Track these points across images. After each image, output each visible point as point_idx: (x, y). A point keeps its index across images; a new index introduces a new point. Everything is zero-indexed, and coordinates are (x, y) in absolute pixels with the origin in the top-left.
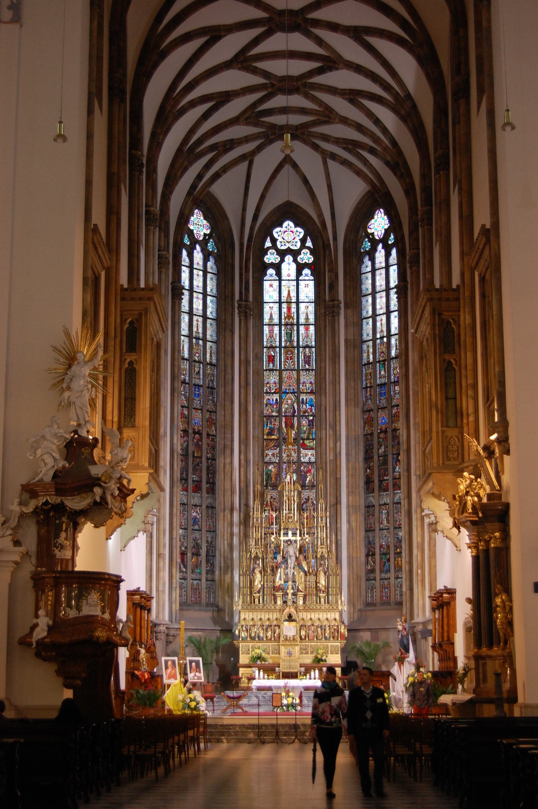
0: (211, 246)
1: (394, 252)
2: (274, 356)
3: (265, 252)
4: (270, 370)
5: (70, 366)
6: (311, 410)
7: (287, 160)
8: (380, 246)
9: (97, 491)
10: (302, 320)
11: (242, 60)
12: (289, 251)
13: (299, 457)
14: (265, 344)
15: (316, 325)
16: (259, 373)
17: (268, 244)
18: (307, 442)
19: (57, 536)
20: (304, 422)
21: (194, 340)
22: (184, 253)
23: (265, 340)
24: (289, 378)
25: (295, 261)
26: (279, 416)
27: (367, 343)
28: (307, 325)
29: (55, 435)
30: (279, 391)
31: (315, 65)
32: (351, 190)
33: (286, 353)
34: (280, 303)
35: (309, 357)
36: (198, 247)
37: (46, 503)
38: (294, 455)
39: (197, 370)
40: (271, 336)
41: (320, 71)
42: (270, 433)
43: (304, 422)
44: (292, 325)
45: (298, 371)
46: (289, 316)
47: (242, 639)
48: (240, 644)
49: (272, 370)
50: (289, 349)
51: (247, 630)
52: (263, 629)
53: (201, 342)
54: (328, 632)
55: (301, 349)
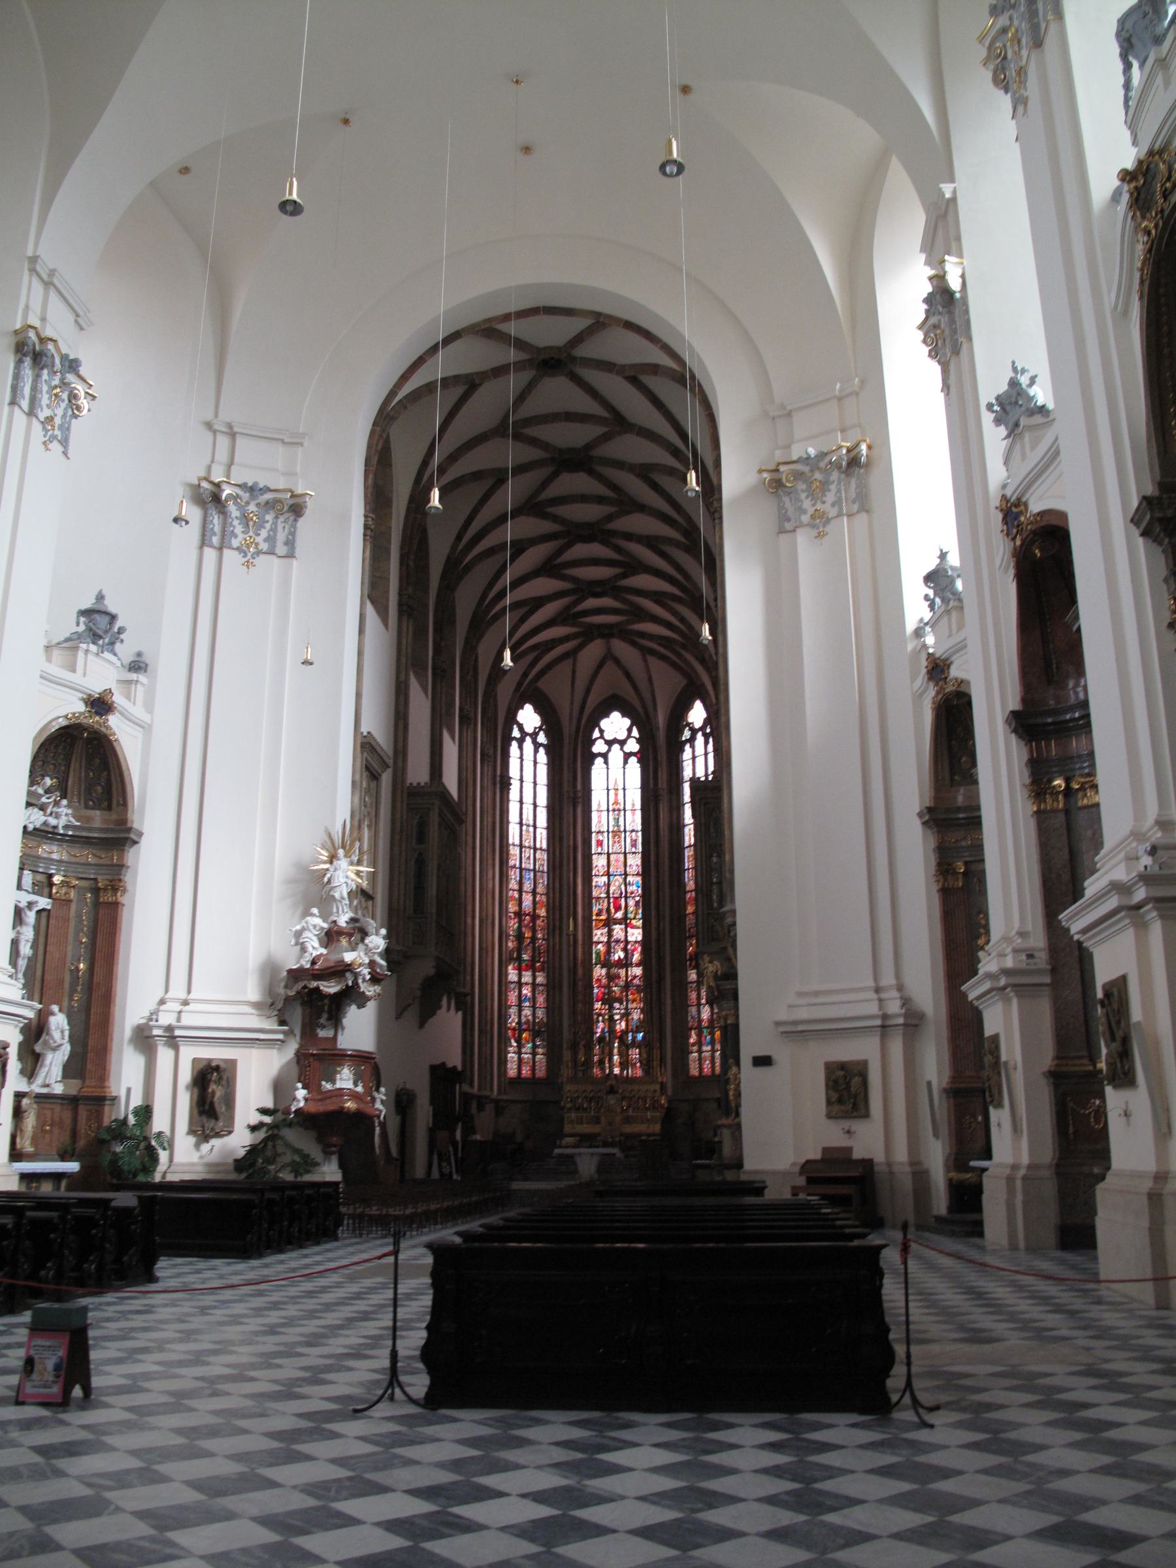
0: (542, 738)
1: (711, 740)
3: (593, 742)
5: (331, 863)
7: (609, 657)
8: (700, 733)
9: (348, 975)
10: (628, 807)
11: (548, 568)
12: (615, 741)
13: (626, 936)
14: (593, 829)
15: (642, 809)
16: (588, 857)
17: (596, 734)
18: (634, 922)
19: (320, 1017)
20: (631, 903)
21: (524, 828)
22: (514, 744)
24: (617, 861)
25: (622, 749)
26: (608, 897)
28: (633, 810)
29: (315, 926)
30: (608, 874)
31: (617, 571)
32: (666, 682)
33: (614, 837)
34: (608, 790)
36: (528, 739)
37: (305, 987)
38: (621, 935)
41: (624, 576)
42: (599, 914)
43: (631, 903)
45: (625, 854)
46: (616, 803)
50: (616, 833)
53: (531, 829)
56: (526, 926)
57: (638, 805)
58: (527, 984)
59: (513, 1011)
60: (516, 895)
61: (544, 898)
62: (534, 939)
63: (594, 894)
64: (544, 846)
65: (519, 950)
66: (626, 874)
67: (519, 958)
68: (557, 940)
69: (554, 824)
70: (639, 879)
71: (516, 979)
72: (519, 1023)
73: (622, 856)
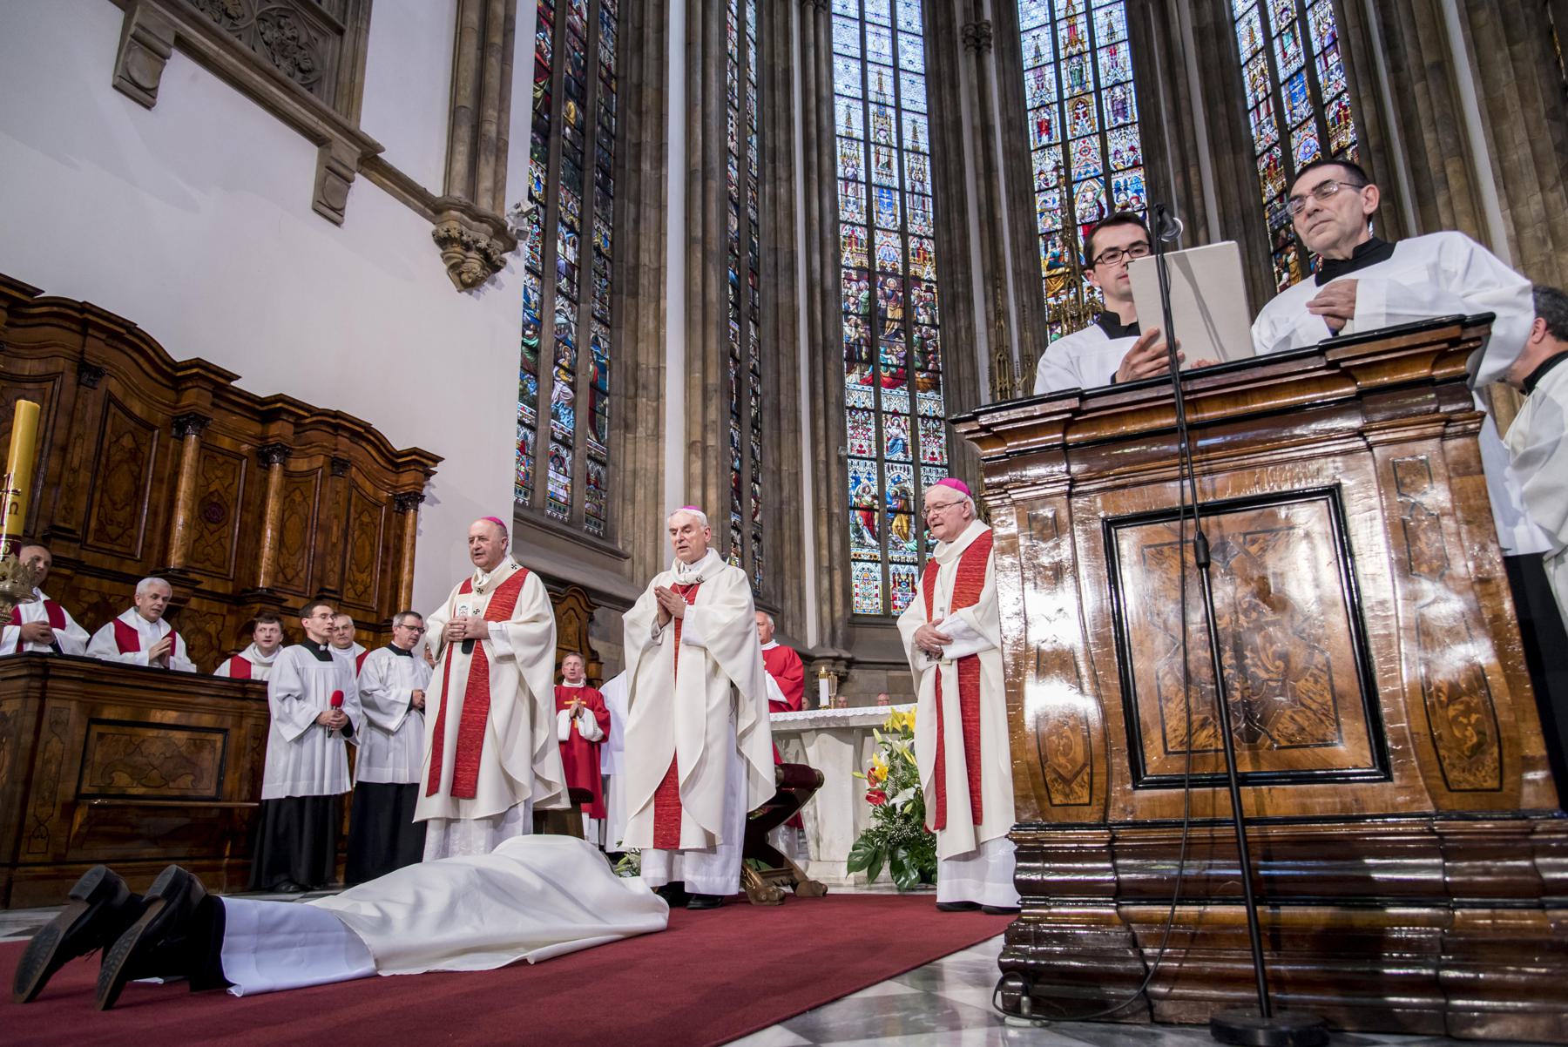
2: (1049, 121)
4: (1043, 148)
6: (1138, 199)
10: (1101, 40)
14: (1029, 105)
15: (1133, 39)
21: (873, 108)
23: (1028, 95)
27: (1246, 18)
28: (1112, 48)
35: (1124, 102)
39: (883, 159)
40: (1040, 87)
44: (1080, 54)
45: (1102, 134)
46: (1074, 41)
49: (1049, 146)
53: (891, 112)
55: (1104, 93)
56: (887, 298)
57: (1122, 31)
58: (896, 413)
59: (863, 470)
60: (862, 234)
61: (929, 246)
62: (908, 323)
63: (1043, 224)
64: (924, 146)
65: (873, 345)
66: (1108, 172)
67: (872, 359)
68: (962, 323)
69: (940, 100)
70: (1140, 173)
71: (870, 404)
72: (881, 496)
73: (1096, 140)
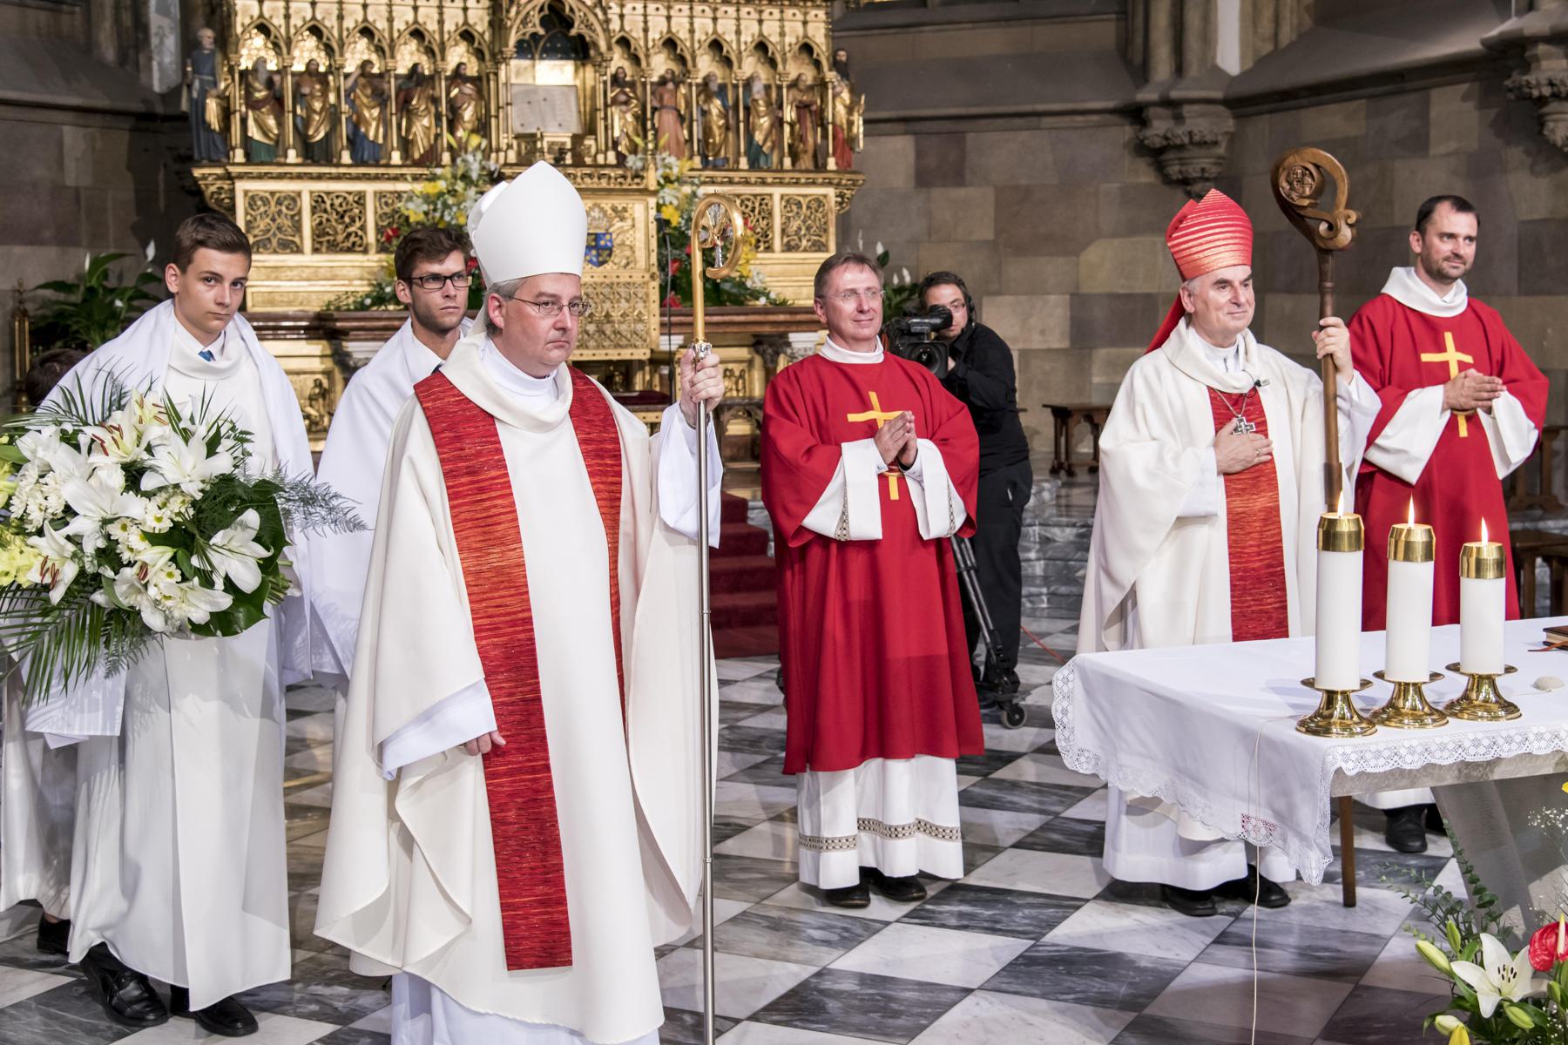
47: (249, 159)
48: (241, 186)
51: (277, 101)
52: (380, 98)
54: (765, 122)
